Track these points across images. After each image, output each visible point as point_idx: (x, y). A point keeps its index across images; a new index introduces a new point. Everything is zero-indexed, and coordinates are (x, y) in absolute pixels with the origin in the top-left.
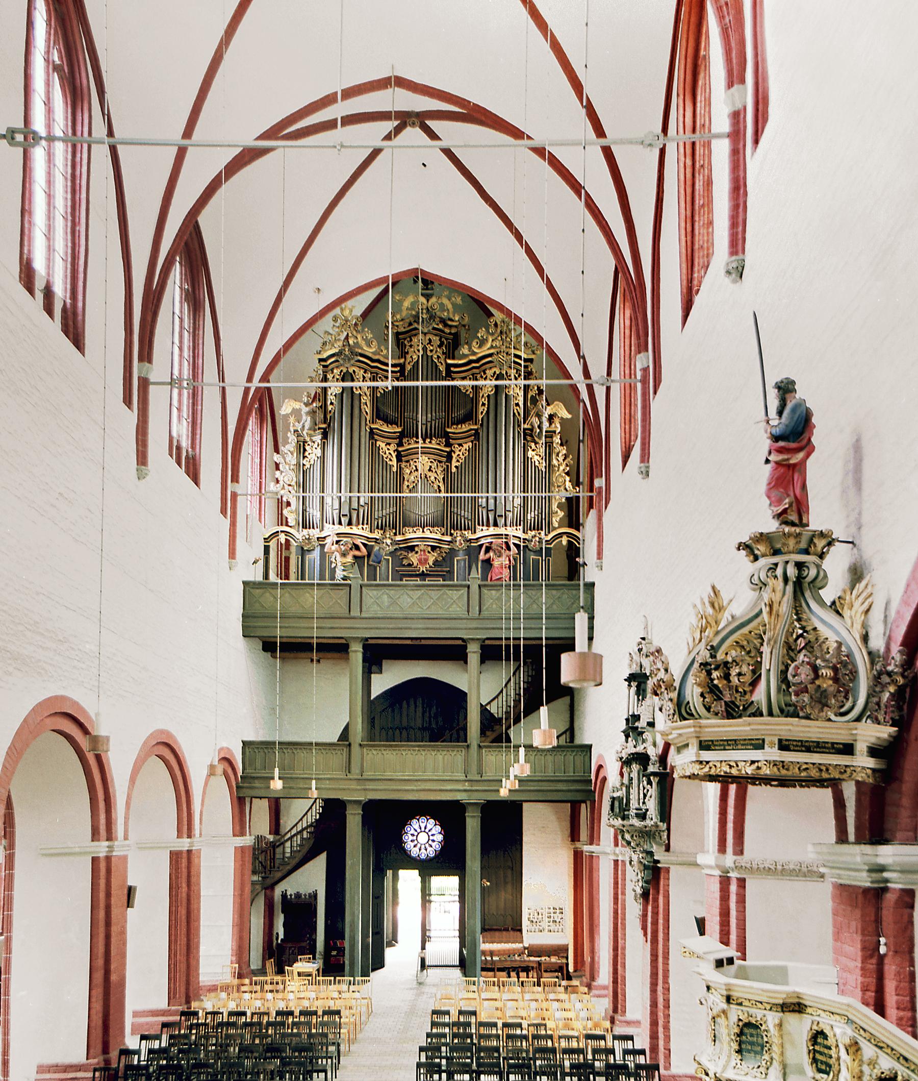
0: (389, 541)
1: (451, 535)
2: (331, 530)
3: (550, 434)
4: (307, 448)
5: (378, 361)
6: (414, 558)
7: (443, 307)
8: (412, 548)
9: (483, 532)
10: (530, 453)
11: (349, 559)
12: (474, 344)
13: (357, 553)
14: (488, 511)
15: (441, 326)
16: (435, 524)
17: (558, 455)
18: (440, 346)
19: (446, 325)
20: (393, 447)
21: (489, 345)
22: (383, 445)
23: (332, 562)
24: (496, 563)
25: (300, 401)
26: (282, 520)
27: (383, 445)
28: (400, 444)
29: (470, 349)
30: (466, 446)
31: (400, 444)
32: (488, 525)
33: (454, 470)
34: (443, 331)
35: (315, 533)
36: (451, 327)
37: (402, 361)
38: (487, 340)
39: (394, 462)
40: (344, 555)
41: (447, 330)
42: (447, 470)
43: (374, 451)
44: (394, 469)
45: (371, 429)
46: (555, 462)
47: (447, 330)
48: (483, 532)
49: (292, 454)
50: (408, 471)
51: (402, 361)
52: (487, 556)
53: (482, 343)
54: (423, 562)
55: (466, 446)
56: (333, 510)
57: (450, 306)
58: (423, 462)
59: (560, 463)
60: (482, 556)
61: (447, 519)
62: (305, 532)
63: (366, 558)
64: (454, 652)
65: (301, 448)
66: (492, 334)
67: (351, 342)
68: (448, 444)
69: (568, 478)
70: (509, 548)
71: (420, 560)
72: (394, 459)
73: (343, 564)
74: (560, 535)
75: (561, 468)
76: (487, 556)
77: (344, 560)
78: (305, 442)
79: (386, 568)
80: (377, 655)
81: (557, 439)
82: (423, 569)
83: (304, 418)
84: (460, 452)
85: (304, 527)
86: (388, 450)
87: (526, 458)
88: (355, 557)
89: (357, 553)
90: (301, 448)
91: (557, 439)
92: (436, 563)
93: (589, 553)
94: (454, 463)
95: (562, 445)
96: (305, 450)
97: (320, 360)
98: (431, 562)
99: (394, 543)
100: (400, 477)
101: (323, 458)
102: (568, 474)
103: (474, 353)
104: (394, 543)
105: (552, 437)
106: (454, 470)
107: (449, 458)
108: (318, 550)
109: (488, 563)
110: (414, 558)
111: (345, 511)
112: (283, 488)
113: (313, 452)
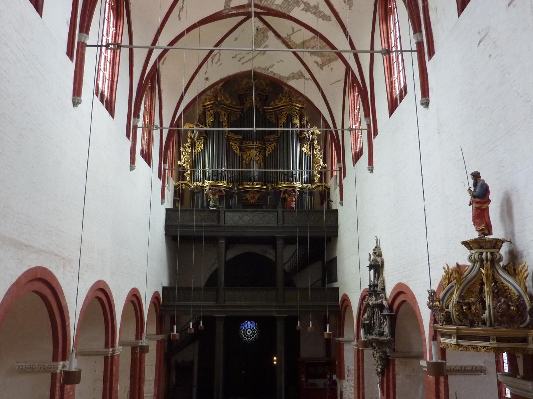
0: (236, 188)
1: (266, 185)
2: (207, 183)
3: (313, 140)
4: (197, 145)
5: (231, 107)
6: (248, 196)
7: (261, 83)
8: (247, 192)
9: (283, 185)
10: (303, 149)
11: (217, 197)
12: (276, 101)
13: (220, 194)
14: (284, 175)
15: (261, 93)
16: (258, 180)
17: (316, 149)
18: (260, 101)
19: (263, 92)
20: (238, 145)
21: (283, 101)
22: (233, 144)
23: (208, 198)
24: (289, 199)
25: (194, 124)
26: (184, 178)
27: (233, 144)
28: (241, 144)
29: (274, 103)
30: (273, 145)
31: (241, 144)
32: (284, 181)
33: (267, 155)
34: (262, 95)
35: (200, 184)
36: (265, 92)
37: (242, 107)
38: (282, 99)
39: (238, 152)
40: (214, 195)
41: (264, 94)
42: (264, 156)
43: (229, 147)
44: (239, 155)
45: (227, 136)
46: (315, 152)
47: (264, 94)
48: (283, 185)
49: (189, 147)
50: (245, 156)
51: (242, 107)
52: (284, 196)
53: (280, 100)
54: (253, 198)
55: (273, 145)
56: (209, 173)
57: (264, 84)
58: (254, 151)
59: (318, 152)
60: (282, 195)
61: (263, 178)
62: (195, 184)
63: (225, 197)
64: (271, 241)
65: (193, 145)
66: (285, 97)
67: (219, 99)
68: (264, 144)
69: (321, 160)
70: (295, 192)
71: (251, 197)
72: (238, 150)
73: (214, 199)
74: (318, 186)
75: (318, 155)
76: (284, 196)
77: (214, 197)
78: (195, 142)
79: (234, 201)
80: (232, 241)
81: (316, 142)
82: (252, 201)
83: (195, 131)
84: (271, 147)
85: (194, 181)
86: (235, 147)
87: (301, 151)
88: (219, 196)
89: (220, 194)
90: (193, 145)
91: (316, 142)
92: (259, 198)
93: (335, 195)
94: (267, 153)
95: (318, 145)
96: (195, 146)
97: (203, 106)
98: (256, 197)
99: (238, 189)
100: (241, 159)
101: (204, 150)
102: (321, 158)
103: (276, 105)
104: (238, 189)
105: (313, 141)
106: (267, 155)
107: (265, 150)
108: (201, 193)
109: (285, 199)
110: (248, 196)
111: (215, 174)
112: (184, 163)
113: (200, 147)
